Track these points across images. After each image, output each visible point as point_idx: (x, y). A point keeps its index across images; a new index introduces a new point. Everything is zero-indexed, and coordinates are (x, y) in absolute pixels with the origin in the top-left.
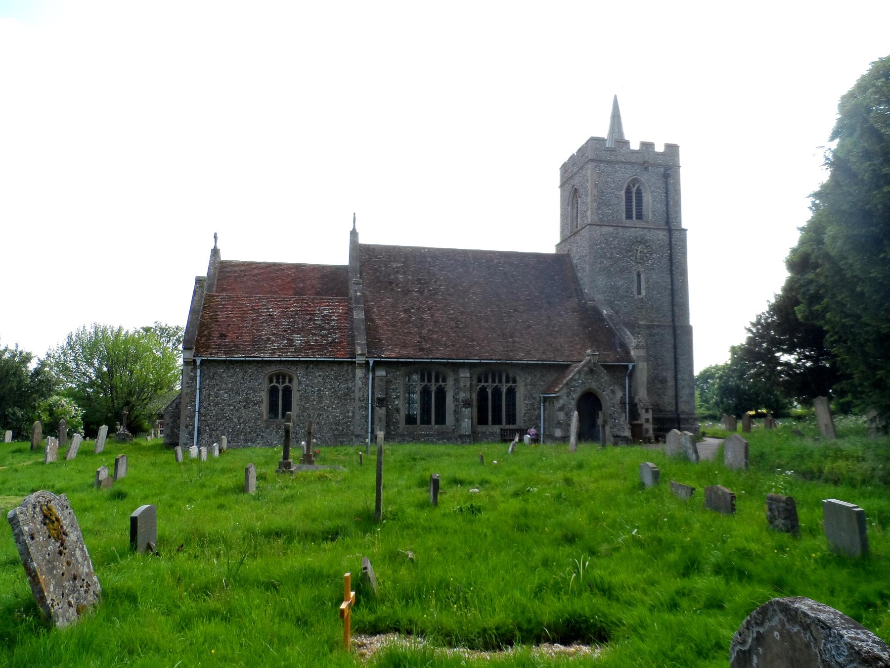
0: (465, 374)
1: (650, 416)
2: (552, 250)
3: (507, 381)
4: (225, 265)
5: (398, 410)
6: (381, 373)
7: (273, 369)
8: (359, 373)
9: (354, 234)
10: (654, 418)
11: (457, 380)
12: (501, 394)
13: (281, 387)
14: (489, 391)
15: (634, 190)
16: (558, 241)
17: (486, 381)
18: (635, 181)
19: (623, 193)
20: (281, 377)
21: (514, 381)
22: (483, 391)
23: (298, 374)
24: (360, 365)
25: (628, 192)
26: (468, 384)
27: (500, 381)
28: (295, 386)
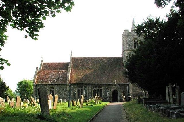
0: (90, 87)
1: (132, 95)
2: (120, 56)
3: (100, 88)
4: (44, 64)
5: (76, 94)
6: (72, 86)
7: (50, 86)
8: (68, 87)
9: (71, 55)
10: (133, 96)
11: (88, 88)
12: (99, 91)
13: (52, 90)
14: (96, 90)
15: (136, 41)
16: (122, 53)
17: (95, 88)
18: (136, 39)
19: (133, 42)
20: (52, 88)
21: (102, 88)
22: (95, 90)
23: (55, 87)
24: (68, 85)
25: (135, 42)
26: (91, 89)
27: (99, 88)
28: (55, 90)
